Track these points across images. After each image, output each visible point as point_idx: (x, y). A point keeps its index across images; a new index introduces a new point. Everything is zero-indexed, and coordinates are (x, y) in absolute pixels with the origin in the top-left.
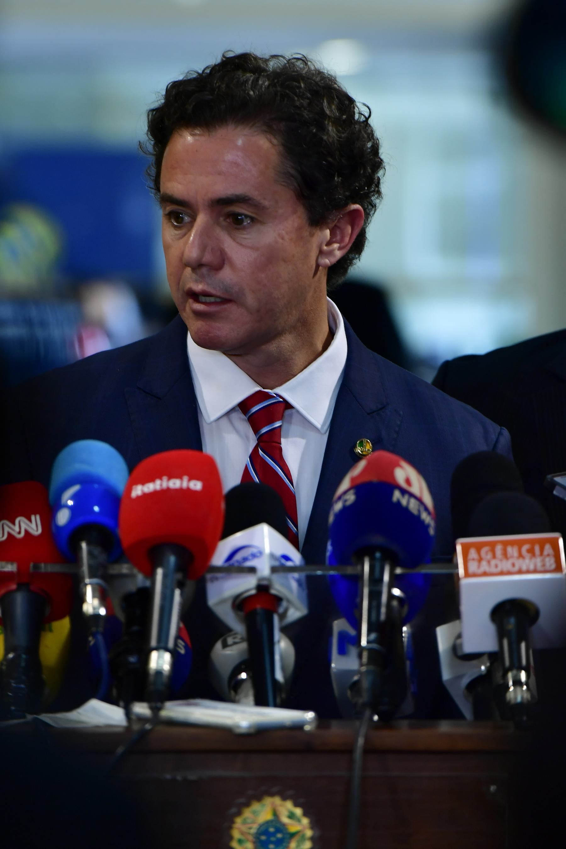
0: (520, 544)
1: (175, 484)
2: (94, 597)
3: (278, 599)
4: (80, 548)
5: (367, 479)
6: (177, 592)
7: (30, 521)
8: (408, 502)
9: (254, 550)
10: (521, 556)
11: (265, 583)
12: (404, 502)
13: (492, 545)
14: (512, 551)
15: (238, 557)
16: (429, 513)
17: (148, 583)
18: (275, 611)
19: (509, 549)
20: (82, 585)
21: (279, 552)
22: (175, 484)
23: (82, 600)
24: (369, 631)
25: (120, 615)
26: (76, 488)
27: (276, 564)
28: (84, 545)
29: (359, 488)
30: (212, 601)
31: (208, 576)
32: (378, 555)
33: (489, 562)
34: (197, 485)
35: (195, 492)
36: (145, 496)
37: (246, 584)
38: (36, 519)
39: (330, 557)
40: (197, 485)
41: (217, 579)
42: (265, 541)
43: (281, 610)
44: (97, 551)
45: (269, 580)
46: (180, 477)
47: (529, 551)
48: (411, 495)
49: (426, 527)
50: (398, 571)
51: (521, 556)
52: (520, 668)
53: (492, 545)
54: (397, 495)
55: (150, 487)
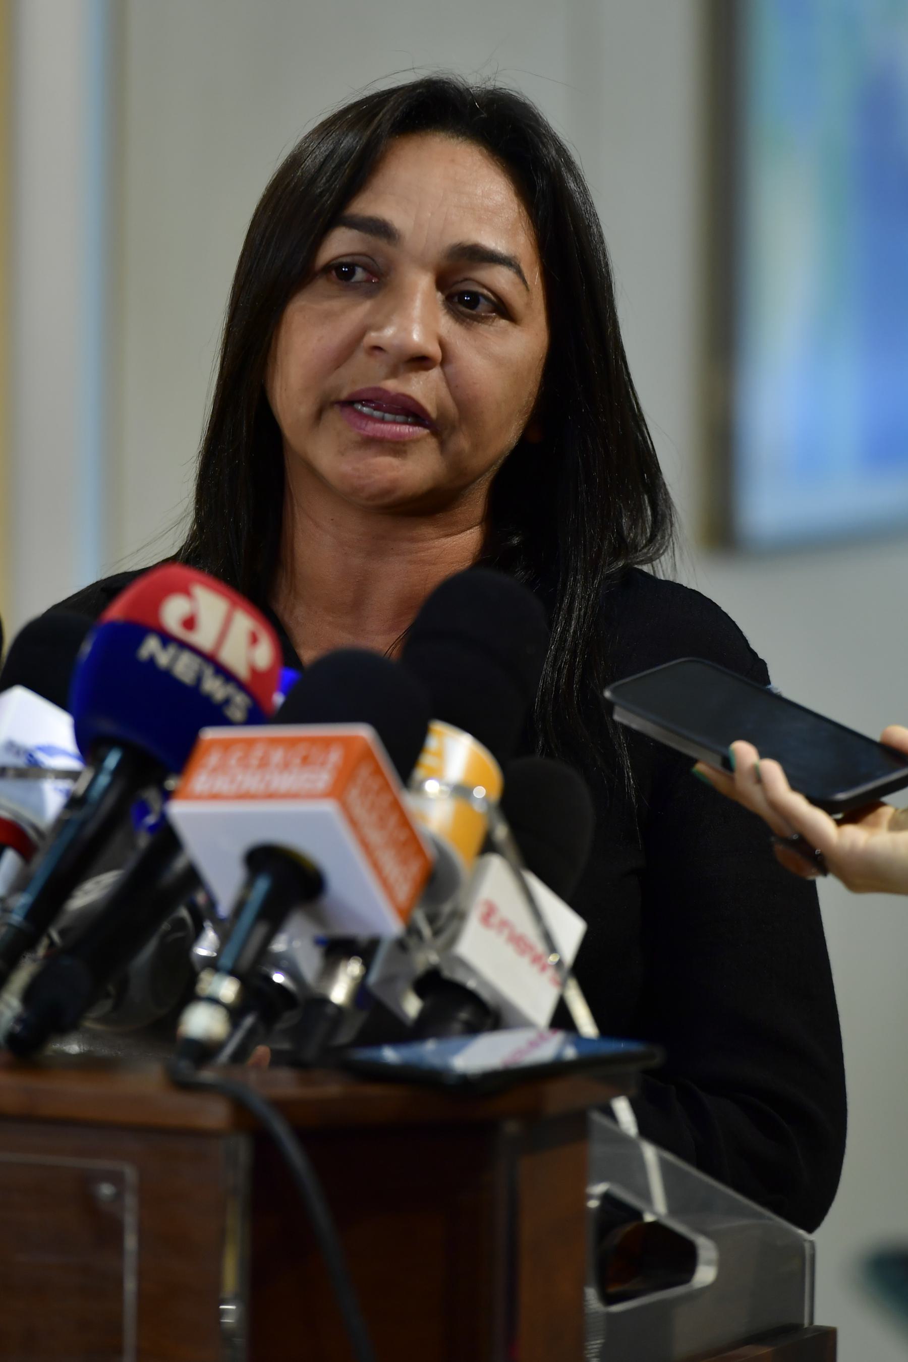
0: (292, 743)
8: (174, 660)
10: (286, 766)
12: (163, 658)
13: (250, 743)
14: (277, 756)
48: (184, 646)
52: (233, 973)
54: (151, 646)
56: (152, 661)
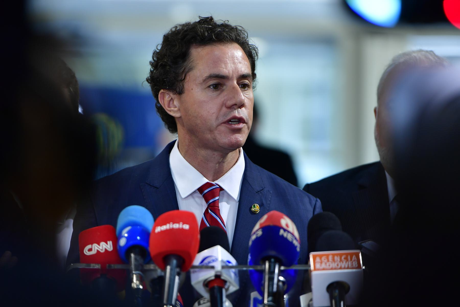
1: (176, 226)
2: (137, 280)
3: (225, 282)
4: (131, 256)
5: (267, 224)
6: (177, 278)
7: (107, 243)
8: (287, 235)
9: (214, 258)
11: (219, 274)
12: (285, 235)
15: (206, 261)
16: (297, 241)
17: (163, 274)
18: (223, 287)
19: (336, 258)
20: (131, 274)
21: (225, 259)
22: (176, 226)
23: (132, 281)
24: (269, 296)
25: (150, 290)
26: (129, 228)
27: (224, 264)
28: (132, 255)
29: (264, 229)
30: (193, 282)
31: (192, 270)
32: (273, 260)
33: (326, 264)
34: (186, 227)
35: (185, 230)
36: (162, 232)
37: (209, 275)
38: (110, 243)
39: (250, 262)
40: (186, 227)
41: (196, 272)
42: (219, 254)
43: (226, 287)
44: (139, 258)
45: (220, 272)
46: (178, 223)
47: (345, 258)
48: (289, 232)
49: (295, 247)
50: (282, 268)
51: (341, 260)
53: (327, 256)
54: (282, 232)
55: (164, 228)
56: (282, 236)
